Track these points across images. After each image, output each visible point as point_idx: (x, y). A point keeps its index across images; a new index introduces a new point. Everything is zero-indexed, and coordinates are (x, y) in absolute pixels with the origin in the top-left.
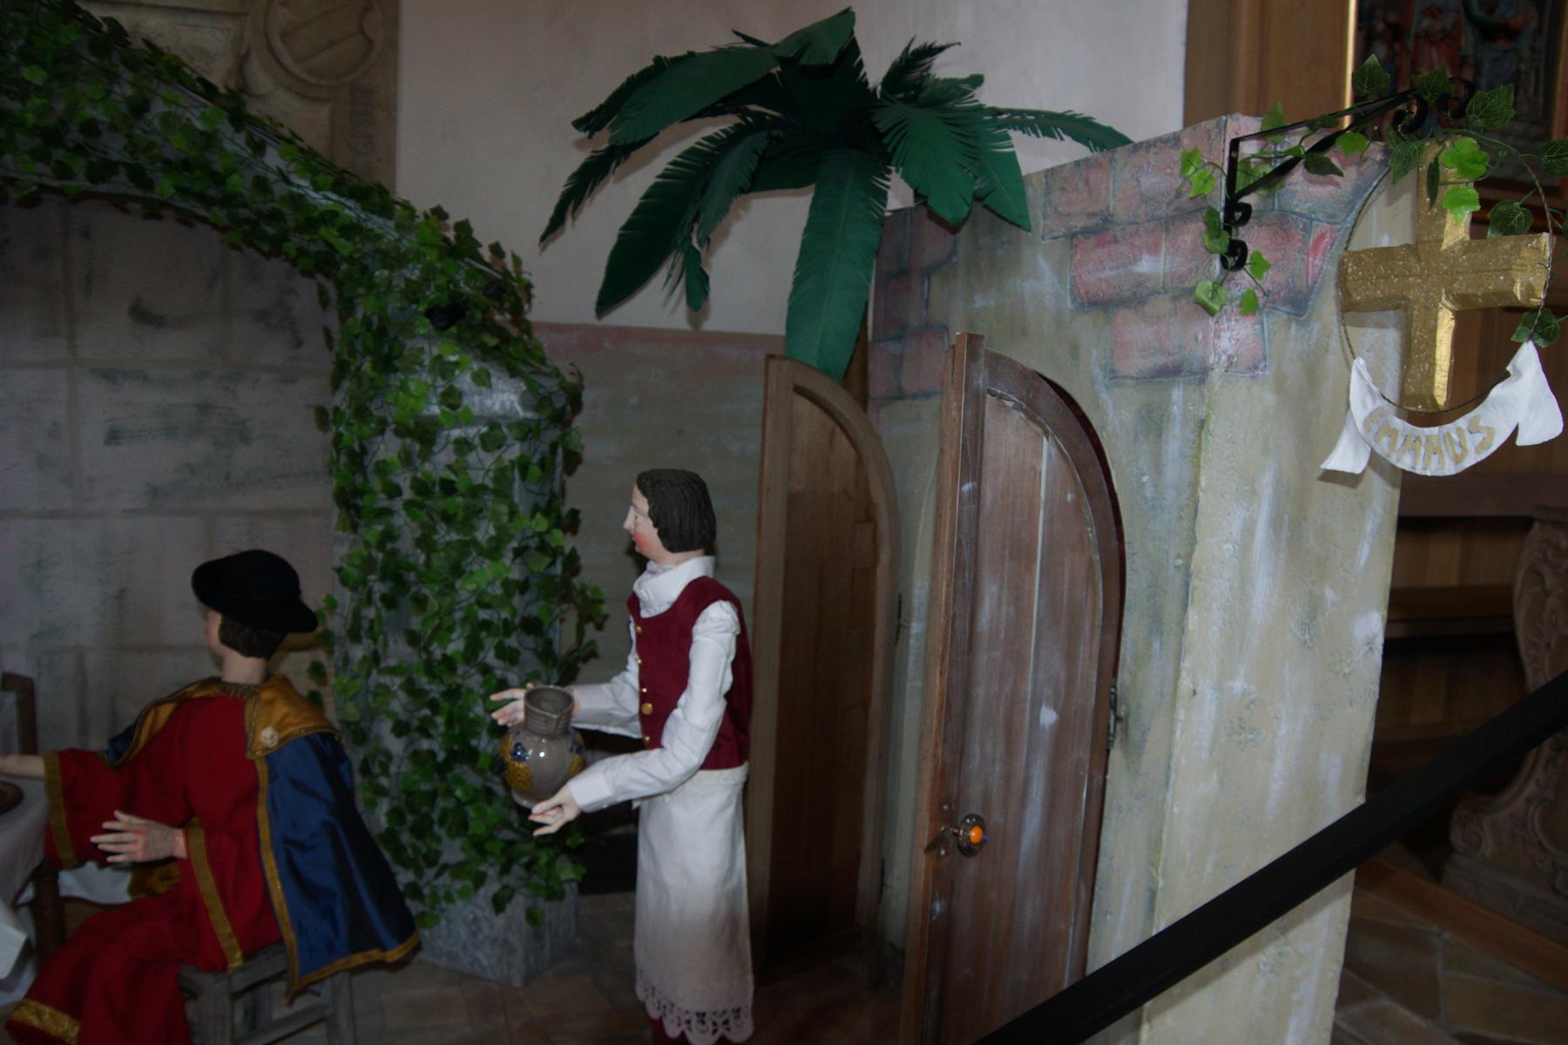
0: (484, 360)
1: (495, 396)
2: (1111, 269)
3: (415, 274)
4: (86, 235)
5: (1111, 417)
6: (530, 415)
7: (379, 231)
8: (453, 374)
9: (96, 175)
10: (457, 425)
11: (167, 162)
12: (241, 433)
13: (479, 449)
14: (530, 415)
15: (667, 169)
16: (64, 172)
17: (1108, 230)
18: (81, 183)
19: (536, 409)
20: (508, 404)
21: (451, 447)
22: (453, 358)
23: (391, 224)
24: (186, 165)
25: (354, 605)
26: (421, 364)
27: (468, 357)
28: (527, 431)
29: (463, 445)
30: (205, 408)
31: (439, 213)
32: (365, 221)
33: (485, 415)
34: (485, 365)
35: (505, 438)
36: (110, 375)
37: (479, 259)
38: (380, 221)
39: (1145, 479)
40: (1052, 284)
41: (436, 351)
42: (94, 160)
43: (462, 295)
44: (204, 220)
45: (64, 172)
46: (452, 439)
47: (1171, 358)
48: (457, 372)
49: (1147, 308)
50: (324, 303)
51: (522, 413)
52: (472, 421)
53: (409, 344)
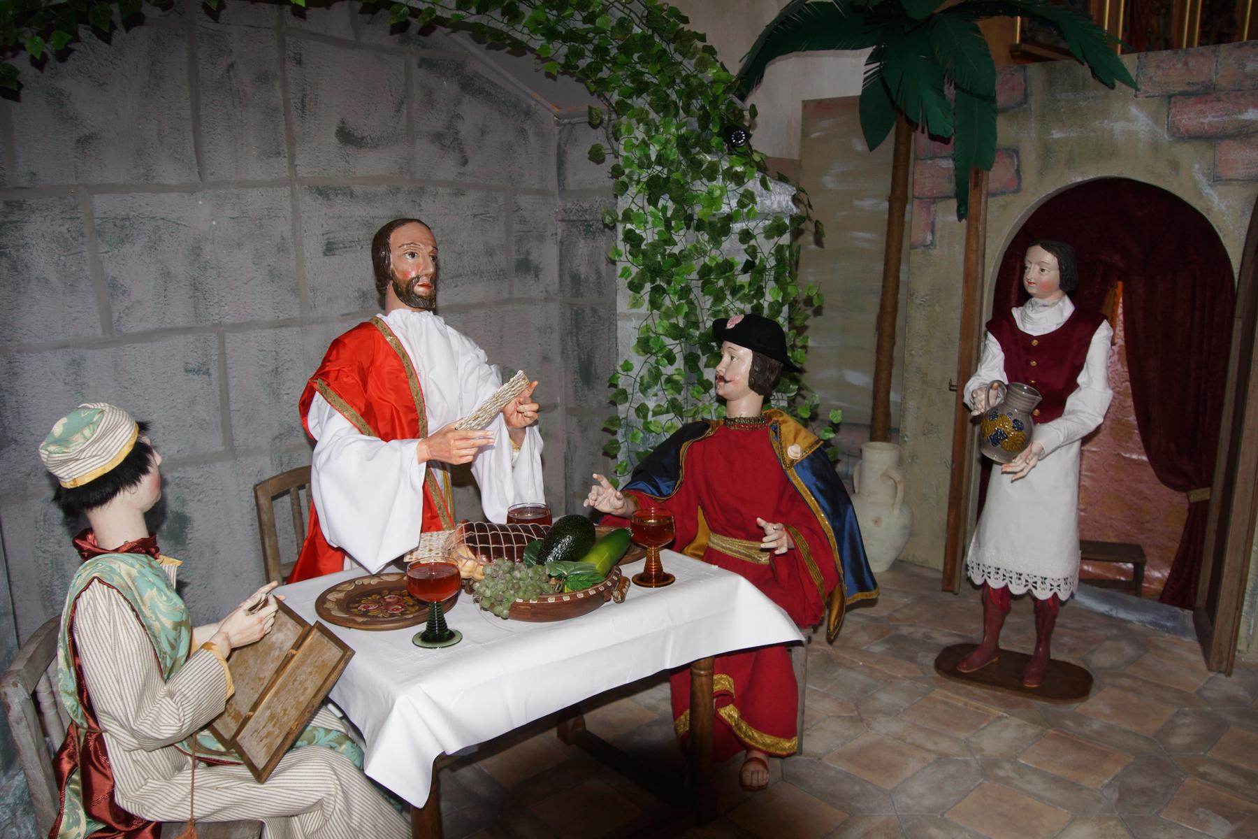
1: (773, 197)
2: (1213, 117)
4: (299, 62)
5: (1216, 203)
20: (784, 203)
22: (739, 169)
23: (685, 62)
25: (647, 366)
29: (746, 236)
33: (766, 211)
36: (323, 192)
41: (725, 165)
44: (533, 50)
48: (746, 180)
51: (795, 210)
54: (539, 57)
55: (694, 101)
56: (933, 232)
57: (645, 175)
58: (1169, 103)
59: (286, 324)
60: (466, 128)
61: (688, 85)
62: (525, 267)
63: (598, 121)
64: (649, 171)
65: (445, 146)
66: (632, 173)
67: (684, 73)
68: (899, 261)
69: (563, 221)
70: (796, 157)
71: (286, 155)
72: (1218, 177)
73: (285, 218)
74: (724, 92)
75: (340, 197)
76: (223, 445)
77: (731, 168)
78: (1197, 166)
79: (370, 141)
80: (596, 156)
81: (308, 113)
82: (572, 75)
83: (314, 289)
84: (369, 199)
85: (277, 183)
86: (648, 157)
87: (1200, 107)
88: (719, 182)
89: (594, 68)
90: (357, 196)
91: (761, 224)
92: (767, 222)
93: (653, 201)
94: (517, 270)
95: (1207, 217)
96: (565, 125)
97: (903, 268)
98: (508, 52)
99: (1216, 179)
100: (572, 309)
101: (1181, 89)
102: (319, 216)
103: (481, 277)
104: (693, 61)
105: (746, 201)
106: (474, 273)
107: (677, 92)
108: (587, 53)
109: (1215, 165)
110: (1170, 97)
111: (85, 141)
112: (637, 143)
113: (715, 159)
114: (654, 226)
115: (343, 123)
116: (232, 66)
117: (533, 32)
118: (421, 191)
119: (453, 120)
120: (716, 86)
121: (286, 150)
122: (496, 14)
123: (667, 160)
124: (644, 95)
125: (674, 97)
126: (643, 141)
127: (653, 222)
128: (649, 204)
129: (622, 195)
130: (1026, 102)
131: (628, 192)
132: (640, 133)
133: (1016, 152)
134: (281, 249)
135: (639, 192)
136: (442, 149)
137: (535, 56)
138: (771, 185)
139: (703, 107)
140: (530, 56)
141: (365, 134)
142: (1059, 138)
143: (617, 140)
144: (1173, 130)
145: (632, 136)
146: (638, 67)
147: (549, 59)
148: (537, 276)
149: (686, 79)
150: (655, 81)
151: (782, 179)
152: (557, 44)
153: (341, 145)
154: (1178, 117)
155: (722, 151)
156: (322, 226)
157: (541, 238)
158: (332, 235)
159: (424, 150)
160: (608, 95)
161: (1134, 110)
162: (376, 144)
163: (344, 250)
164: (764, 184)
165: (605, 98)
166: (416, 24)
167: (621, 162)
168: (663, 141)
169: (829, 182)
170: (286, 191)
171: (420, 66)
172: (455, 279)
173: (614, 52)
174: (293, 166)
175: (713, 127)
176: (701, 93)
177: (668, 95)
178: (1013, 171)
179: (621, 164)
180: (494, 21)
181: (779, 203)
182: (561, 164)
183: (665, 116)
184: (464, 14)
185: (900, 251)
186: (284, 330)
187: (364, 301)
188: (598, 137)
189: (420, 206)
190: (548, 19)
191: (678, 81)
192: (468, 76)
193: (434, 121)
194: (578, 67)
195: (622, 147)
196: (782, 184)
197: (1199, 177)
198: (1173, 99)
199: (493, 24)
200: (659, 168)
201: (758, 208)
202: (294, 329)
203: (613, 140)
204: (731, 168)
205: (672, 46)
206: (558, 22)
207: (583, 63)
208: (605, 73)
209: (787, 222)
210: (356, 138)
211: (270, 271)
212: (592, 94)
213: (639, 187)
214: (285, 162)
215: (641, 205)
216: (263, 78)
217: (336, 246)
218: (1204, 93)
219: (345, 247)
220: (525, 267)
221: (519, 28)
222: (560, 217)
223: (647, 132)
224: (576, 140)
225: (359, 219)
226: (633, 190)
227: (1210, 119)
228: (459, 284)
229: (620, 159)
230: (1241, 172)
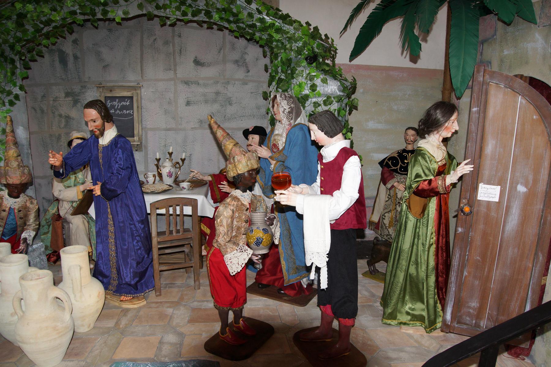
0: (325, 75)
1: (329, 87)
3: (300, 44)
4: (180, 36)
6: (341, 94)
7: (287, 31)
8: (314, 80)
10: (316, 97)
11: (218, 9)
13: (322, 105)
14: (341, 94)
15: (376, 7)
16: (185, 14)
18: (190, 17)
19: (343, 92)
21: (312, 105)
22: (313, 74)
23: (292, 28)
24: (224, 10)
26: (302, 76)
27: (319, 73)
28: (339, 99)
29: (316, 105)
30: (217, 93)
31: (308, 24)
32: (283, 27)
33: (325, 93)
34: (326, 77)
35: (332, 102)
36: (187, 83)
37: (322, 40)
38: (288, 27)
40: (542, 43)
41: (308, 72)
42: (194, 9)
43: (315, 52)
44: (227, 28)
45: (185, 14)
46: (313, 102)
48: (315, 79)
50: (265, 56)
51: (339, 93)
52: (320, 95)
53: (299, 69)
57: (277, 78)
59: (169, 130)
60: (249, 58)
65: (239, 65)
75: (194, 85)
76: (144, 169)
77: (309, 73)
79: (206, 64)
83: (181, 118)
84: (205, 85)
85: (170, 80)
90: (200, 85)
91: (324, 99)
106: (250, 116)
111: (105, 67)
115: (196, 57)
116: (155, 39)
118: (228, 83)
121: (173, 68)
122: (202, 15)
129: (271, 85)
133: (490, 63)
134: (169, 103)
135: (276, 84)
142: (506, 55)
159: (230, 66)
162: (209, 65)
164: (324, 81)
170: (172, 82)
172: (241, 118)
186: (169, 131)
189: (227, 88)
193: (236, 56)
202: (173, 131)
210: (201, 63)
211: (165, 111)
214: (172, 72)
216: (166, 43)
225: (200, 93)
228: (243, 119)
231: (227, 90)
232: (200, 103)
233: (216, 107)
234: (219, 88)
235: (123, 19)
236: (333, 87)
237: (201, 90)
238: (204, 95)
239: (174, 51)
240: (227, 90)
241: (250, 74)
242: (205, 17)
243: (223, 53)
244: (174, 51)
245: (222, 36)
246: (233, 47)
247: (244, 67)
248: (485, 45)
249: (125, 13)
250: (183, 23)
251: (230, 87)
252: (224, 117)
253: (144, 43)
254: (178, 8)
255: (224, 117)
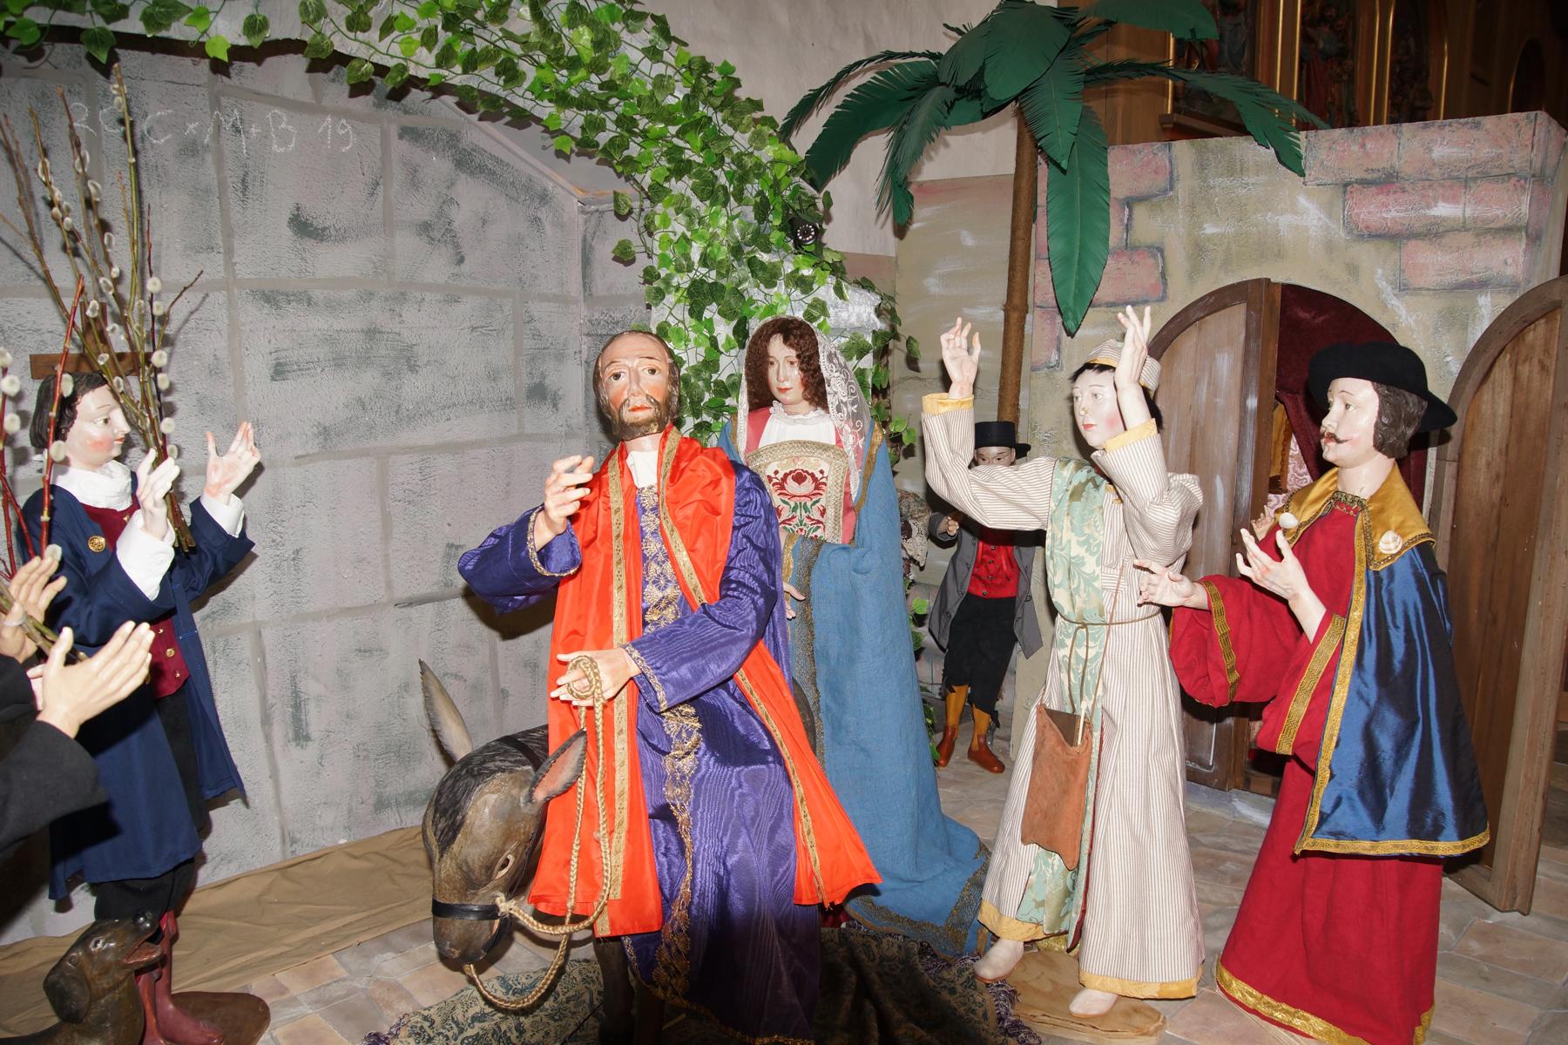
1: (850, 308)
9: (470, 64)
12: (408, 360)
16: (445, 59)
17: (1394, 183)
20: (865, 316)
22: (807, 272)
23: (738, 136)
30: (372, 333)
33: (842, 326)
36: (271, 298)
39: (1448, 359)
41: (788, 268)
44: (538, 121)
47: (1474, 276)
48: (815, 286)
49: (1444, 241)
51: (880, 325)
54: (547, 130)
55: (748, 186)
56: (1059, 350)
57: (683, 280)
58: (1345, 192)
60: (461, 217)
61: (740, 165)
62: (539, 393)
63: (626, 211)
64: (691, 275)
65: (433, 240)
66: (670, 277)
67: (735, 150)
68: (1018, 385)
69: (588, 335)
70: (893, 254)
71: (222, 250)
72: (1404, 285)
73: (219, 331)
74: (787, 175)
75: (294, 303)
78: (1380, 271)
80: (624, 256)
81: (251, 196)
82: (591, 156)
84: (332, 306)
86: (687, 257)
87: (1382, 198)
88: (780, 288)
89: (618, 144)
92: (843, 340)
93: (696, 312)
94: (528, 397)
95: (1393, 334)
96: (592, 213)
97: (1023, 394)
98: (507, 124)
99: (1403, 288)
100: (601, 448)
101: (1358, 176)
102: (265, 329)
103: (481, 407)
104: (748, 135)
105: (815, 313)
107: (726, 173)
108: (610, 125)
109: (1402, 271)
110: (1346, 185)
112: (675, 239)
113: (775, 259)
114: (698, 345)
115: (298, 209)
117: (539, 97)
118: (402, 297)
119: (444, 207)
120: (777, 166)
122: (488, 72)
123: (714, 260)
124: (686, 178)
125: (723, 180)
126: (684, 236)
127: (696, 339)
128: (691, 315)
129: (657, 305)
130: (1172, 189)
131: (664, 301)
132: (679, 226)
133: (1161, 250)
134: (214, 372)
135: (679, 301)
136: (429, 243)
137: (543, 129)
138: (849, 292)
139: (760, 193)
140: (535, 129)
141: (328, 224)
142: (1213, 234)
143: (651, 234)
144: (1350, 225)
145: (670, 229)
146: (676, 141)
147: (561, 132)
148: (555, 405)
149: (738, 160)
150: (700, 160)
151: (865, 284)
152: (570, 113)
153: (295, 238)
154: (1356, 211)
155: (786, 249)
156: (269, 342)
157: (560, 357)
158: (283, 354)
159: (407, 244)
160: (638, 177)
161: (1303, 201)
162: (342, 237)
163: (299, 373)
164: (839, 291)
165: (635, 181)
166: (385, 85)
167: (655, 262)
168: (708, 237)
169: (932, 285)
171: (401, 137)
172: (447, 411)
173: (643, 123)
174: (230, 264)
175: (774, 218)
176: (758, 176)
177: (716, 177)
178: (1157, 273)
179: (656, 266)
180: (486, 83)
181: (859, 316)
182: (586, 262)
183: (712, 205)
184: (446, 73)
185: (1019, 372)
187: (325, 439)
188: (628, 231)
189: (401, 316)
190: (556, 81)
191: (727, 160)
192: (464, 150)
193: (422, 208)
194: (597, 145)
195: (656, 244)
196: (863, 291)
197: (1383, 284)
198: (1349, 188)
199: (485, 87)
200: (704, 270)
201: (831, 322)
203: (645, 235)
204: (797, 270)
205: (720, 116)
206: (570, 84)
207: (603, 138)
208: (634, 150)
209: (869, 339)
210: (316, 229)
212: (619, 175)
213: (679, 294)
214: (220, 259)
215: (681, 318)
216: (191, 149)
217: (288, 368)
218: (1387, 181)
219: (300, 370)
220: (539, 393)
221: (520, 91)
222: (586, 331)
223: (689, 226)
224: (605, 232)
226: (671, 298)
227: (1393, 214)
229: (655, 258)
230: (1431, 279)
231: (402, 322)
232: (319, 370)
233: (370, 379)
234: (377, 314)
235: (237, 53)
236: (862, 309)
237: (318, 323)
238: (330, 340)
239: (222, 184)
240: (402, 322)
241: (465, 268)
242: (495, 80)
243: (384, 197)
244: (222, 184)
245: (378, 141)
246: (414, 179)
247: (450, 246)
248: (1140, 211)
249: (254, 25)
250: (428, 94)
251: (410, 314)
252: (397, 412)
253: (104, 143)
254: (429, 38)
255: (397, 412)
